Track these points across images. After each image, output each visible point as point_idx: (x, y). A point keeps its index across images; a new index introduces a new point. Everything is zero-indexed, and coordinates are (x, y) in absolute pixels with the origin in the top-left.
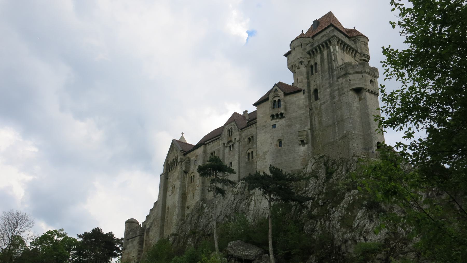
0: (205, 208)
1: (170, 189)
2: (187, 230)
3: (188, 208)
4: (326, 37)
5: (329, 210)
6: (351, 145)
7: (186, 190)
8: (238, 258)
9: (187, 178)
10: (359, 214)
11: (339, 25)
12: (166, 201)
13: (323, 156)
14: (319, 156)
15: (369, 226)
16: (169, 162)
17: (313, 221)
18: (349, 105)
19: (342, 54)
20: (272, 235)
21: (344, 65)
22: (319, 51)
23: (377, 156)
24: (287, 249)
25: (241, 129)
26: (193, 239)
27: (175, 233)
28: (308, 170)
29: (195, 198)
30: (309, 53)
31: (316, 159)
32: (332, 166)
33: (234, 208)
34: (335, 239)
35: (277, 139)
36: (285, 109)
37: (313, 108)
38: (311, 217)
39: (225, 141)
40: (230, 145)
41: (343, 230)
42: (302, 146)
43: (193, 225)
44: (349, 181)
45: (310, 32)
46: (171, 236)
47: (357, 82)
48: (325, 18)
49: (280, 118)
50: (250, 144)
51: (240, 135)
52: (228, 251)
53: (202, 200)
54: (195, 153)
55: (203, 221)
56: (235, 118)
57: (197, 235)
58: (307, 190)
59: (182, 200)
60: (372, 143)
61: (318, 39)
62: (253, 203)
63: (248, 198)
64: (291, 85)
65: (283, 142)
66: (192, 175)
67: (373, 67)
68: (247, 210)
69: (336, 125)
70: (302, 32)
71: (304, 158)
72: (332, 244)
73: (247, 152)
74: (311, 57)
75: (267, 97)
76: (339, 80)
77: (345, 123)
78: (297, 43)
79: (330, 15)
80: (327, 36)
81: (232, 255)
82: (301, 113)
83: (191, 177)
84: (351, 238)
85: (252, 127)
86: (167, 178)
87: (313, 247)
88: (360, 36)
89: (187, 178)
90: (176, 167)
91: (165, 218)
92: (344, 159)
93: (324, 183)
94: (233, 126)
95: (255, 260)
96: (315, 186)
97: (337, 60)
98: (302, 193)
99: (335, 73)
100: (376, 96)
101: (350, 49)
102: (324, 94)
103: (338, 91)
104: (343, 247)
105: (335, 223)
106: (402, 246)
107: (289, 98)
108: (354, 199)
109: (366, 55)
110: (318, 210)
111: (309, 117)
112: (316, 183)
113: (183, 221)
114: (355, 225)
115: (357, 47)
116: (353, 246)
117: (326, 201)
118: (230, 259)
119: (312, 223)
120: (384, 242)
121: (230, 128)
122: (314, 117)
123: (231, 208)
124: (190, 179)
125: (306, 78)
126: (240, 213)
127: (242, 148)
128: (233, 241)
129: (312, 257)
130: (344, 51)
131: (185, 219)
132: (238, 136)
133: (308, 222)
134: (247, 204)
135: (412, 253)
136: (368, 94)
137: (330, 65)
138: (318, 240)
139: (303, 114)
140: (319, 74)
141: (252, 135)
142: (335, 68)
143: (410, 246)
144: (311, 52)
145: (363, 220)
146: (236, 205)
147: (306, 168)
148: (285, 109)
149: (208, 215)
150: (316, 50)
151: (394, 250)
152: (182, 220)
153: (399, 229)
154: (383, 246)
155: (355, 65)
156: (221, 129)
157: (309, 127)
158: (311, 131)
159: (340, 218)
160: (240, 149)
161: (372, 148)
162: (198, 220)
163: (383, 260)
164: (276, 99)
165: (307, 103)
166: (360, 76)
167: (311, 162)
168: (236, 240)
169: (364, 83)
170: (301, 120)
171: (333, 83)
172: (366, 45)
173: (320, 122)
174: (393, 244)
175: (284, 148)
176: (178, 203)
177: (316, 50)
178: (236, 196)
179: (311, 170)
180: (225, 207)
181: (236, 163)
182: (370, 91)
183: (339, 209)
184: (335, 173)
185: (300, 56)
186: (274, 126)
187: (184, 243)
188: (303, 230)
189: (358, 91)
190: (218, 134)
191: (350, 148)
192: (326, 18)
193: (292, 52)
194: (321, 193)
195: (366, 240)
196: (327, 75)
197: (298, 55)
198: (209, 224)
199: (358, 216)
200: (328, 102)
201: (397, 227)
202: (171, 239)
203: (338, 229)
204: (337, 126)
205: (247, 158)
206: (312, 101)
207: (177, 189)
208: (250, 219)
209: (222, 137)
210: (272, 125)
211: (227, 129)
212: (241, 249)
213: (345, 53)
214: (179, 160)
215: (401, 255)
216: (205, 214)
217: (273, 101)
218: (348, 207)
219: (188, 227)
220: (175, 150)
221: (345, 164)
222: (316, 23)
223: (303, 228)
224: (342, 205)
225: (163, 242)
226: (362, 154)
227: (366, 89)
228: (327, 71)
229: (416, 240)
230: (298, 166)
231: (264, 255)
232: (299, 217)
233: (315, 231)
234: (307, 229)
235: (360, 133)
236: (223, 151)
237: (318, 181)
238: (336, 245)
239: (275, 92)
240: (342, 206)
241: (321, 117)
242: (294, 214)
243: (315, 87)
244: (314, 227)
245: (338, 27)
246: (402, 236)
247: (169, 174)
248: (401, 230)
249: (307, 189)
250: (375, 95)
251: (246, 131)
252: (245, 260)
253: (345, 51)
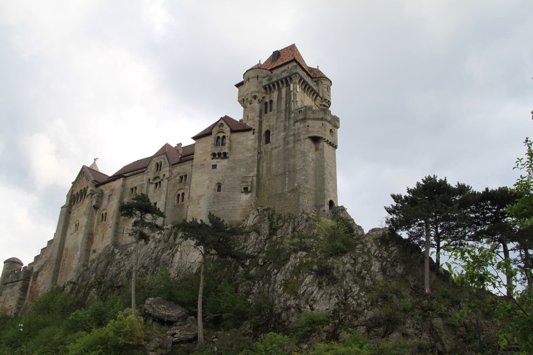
0: (116, 254)
1: (72, 226)
2: (91, 278)
3: (94, 251)
4: (287, 73)
5: (269, 271)
6: (301, 200)
7: (93, 230)
8: (156, 318)
9: (97, 215)
10: (306, 279)
11: (302, 62)
12: (65, 240)
13: (267, 208)
14: (263, 208)
15: (317, 294)
16: (75, 193)
17: (250, 282)
18: (304, 154)
19: (303, 96)
20: (203, 294)
21: (304, 108)
22: (277, 88)
23: (328, 216)
24: (218, 312)
25: (173, 165)
26: (97, 290)
27: (74, 281)
28: (249, 222)
29: (104, 241)
30: (265, 88)
31: (259, 211)
32: (277, 222)
33: (153, 257)
34: (275, 305)
35: (217, 182)
36: (230, 149)
37: (262, 152)
38: (248, 277)
39: (151, 176)
40: (157, 181)
41: (286, 296)
42: (244, 194)
43: (99, 272)
44: (296, 240)
45: (268, 64)
46: (68, 284)
47: (316, 130)
48: (287, 50)
49: (223, 159)
50: (182, 184)
51: (170, 171)
52: (145, 309)
53: (113, 245)
54: (111, 186)
55: (112, 270)
56: (166, 150)
57: (103, 285)
58: (246, 246)
59: (87, 241)
60: (324, 201)
61: (277, 74)
62: (178, 254)
63: (173, 247)
64: (238, 120)
65: (222, 187)
66: (104, 212)
67: (335, 116)
68: (170, 262)
69: (287, 176)
70: (260, 62)
71: (245, 209)
72: (271, 310)
73: (177, 192)
74: (266, 93)
75: (210, 131)
76: (296, 124)
77: (298, 175)
78: (252, 74)
79: (292, 48)
80: (288, 71)
81: (150, 314)
82: (248, 156)
83: (103, 214)
84: (294, 306)
85: (186, 164)
86: (70, 213)
87: (248, 312)
88: (323, 78)
89: (97, 215)
90: (83, 201)
91: (62, 261)
92: (291, 215)
93: (266, 239)
94: (163, 159)
95: (178, 322)
96: (256, 242)
97: (297, 101)
98: (239, 249)
99: (293, 115)
100: (334, 148)
101: (311, 91)
102: (277, 138)
103: (293, 137)
104: (284, 315)
105: (277, 287)
106: (352, 319)
107: (235, 136)
108: (301, 262)
109: (327, 101)
110: (256, 269)
111: (256, 161)
112: (257, 239)
113: (86, 267)
114: (301, 291)
115: (319, 90)
116: (296, 314)
117: (267, 261)
118: (147, 318)
119: (248, 284)
120: (333, 313)
121: (158, 162)
122: (263, 162)
123: (151, 258)
124: (101, 217)
125: (258, 116)
126: (161, 264)
127: (171, 188)
128: (150, 297)
129: (246, 324)
130: (304, 92)
131: (89, 264)
132: (168, 172)
133: (244, 283)
134: (170, 254)
135: (363, 328)
136: (325, 144)
137: (288, 105)
138: (254, 304)
139: (250, 157)
140: (274, 114)
142: (293, 110)
143: (361, 319)
144: (267, 87)
145: (311, 287)
146: (156, 254)
147: (246, 220)
148: (230, 149)
149: (119, 262)
150: (274, 86)
151: (343, 323)
152: (84, 265)
153: (350, 299)
154: (331, 316)
155: (316, 110)
156: (150, 159)
157: (255, 173)
158: (257, 178)
159: (283, 282)
160: (169, 188)
161: (323, 206)
162: (106, 267)
163: (330, 333)
164: (221, 135)
165: (256, 145)
166: (320, 123)
167: (254, 214)
168: (155, 296)
169: (323, 132)
170: (247, 164)
171: (288, 126)
172: (328, 89)
173: (269, 170)
174: (343, 315)
175: (223, 193)
176: (82, 245)
177: (274, 86)
178: (158, 243)
179: (252, 224)
180: (143, 255)
181: (163, 204)
182: (329, 142)
183: (283, 272)
184: (280, 230)
185: (254, 89)
186: (214, 167)
187: (84, 294)
188: (236, 291)
189: (316, 140)
190: (141, 166)
191: (300, 203)
192: (288, 51)
193: (245, 83)
194: (262, 250)
195: (312, 309)
196: (283, 115)
197: (252, 87)
198: (119, 273)
199: (305, 281)
200: (281, 148)
201: (347, 297)
202: (68, 289)
203: (281, 294)
204: (288, 176)
205: (176, 200)
206: (261, 144)
207: (82, 227)
208: (173, 272)
209: (148, 171)
210: (212, 164)
211: (155, 163)
212: (162, 308)
213: (305, 94)
214: (88, 192)
215: (350, 329)
216: (116, 262)
217: (216, 137)
218: (293, 270)
219: (92, 274)
220: (84, 178)
221: (292, 220)
222: (277, 55)
223: (238, 288)
224: (287, 267)
225: (57, 290)
226: (311, 212)
227: (325, 139)
228: (284, 112)
229: (367, 313)
230: (237, 217)
231: (189, 317)
232: (234, 275)
233: (251, 294)
234: (242, 291)
235: (313, 188)
236: (148, 188)
237: (259, 236)
238: (276, 312)
239: (220, 126)
240: (287, 268)
241: (270, 163)
242: (228, 272)
243: (268, 128)
244: (251, 289)
245: (301, 64)
246: (353, 308)
247: (73, 208)
248: (352, 301)
249: (246, 244)
250: (333, 147)
251: (178, 168)
252: (167, 321)
253: (306, 92)
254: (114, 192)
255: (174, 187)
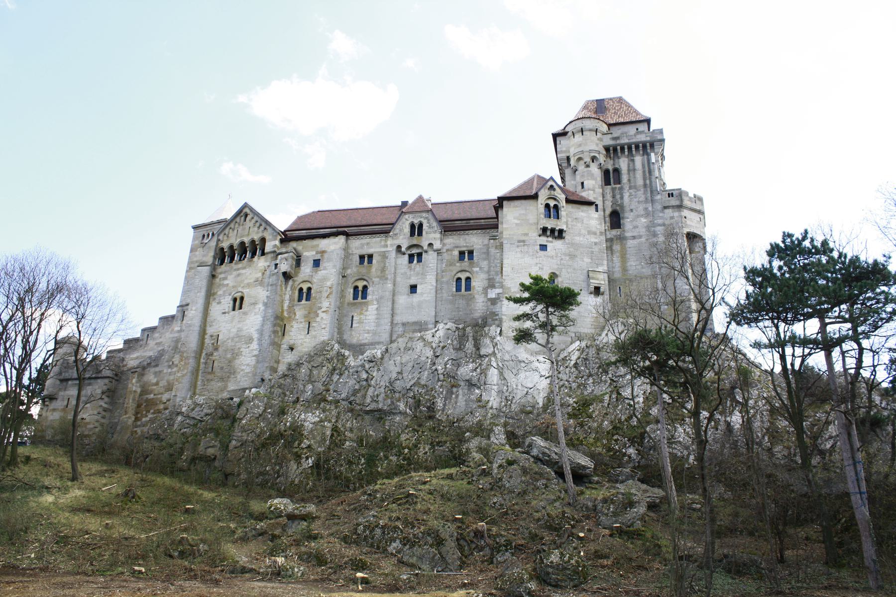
9: (289, 289)
22: (626, 153)
30: (607, 149)
49: (556, 238)
66: (305, 287)
89: (289, 289)
127: (444, 266)
141: (472, 249)
164: (552, 203)
177: (622, 149)
181: (431, 289)
186: (543, 247)
200: (643, 239)
211: (409, 222)
254: (326, 256)
255: (451, 265)
